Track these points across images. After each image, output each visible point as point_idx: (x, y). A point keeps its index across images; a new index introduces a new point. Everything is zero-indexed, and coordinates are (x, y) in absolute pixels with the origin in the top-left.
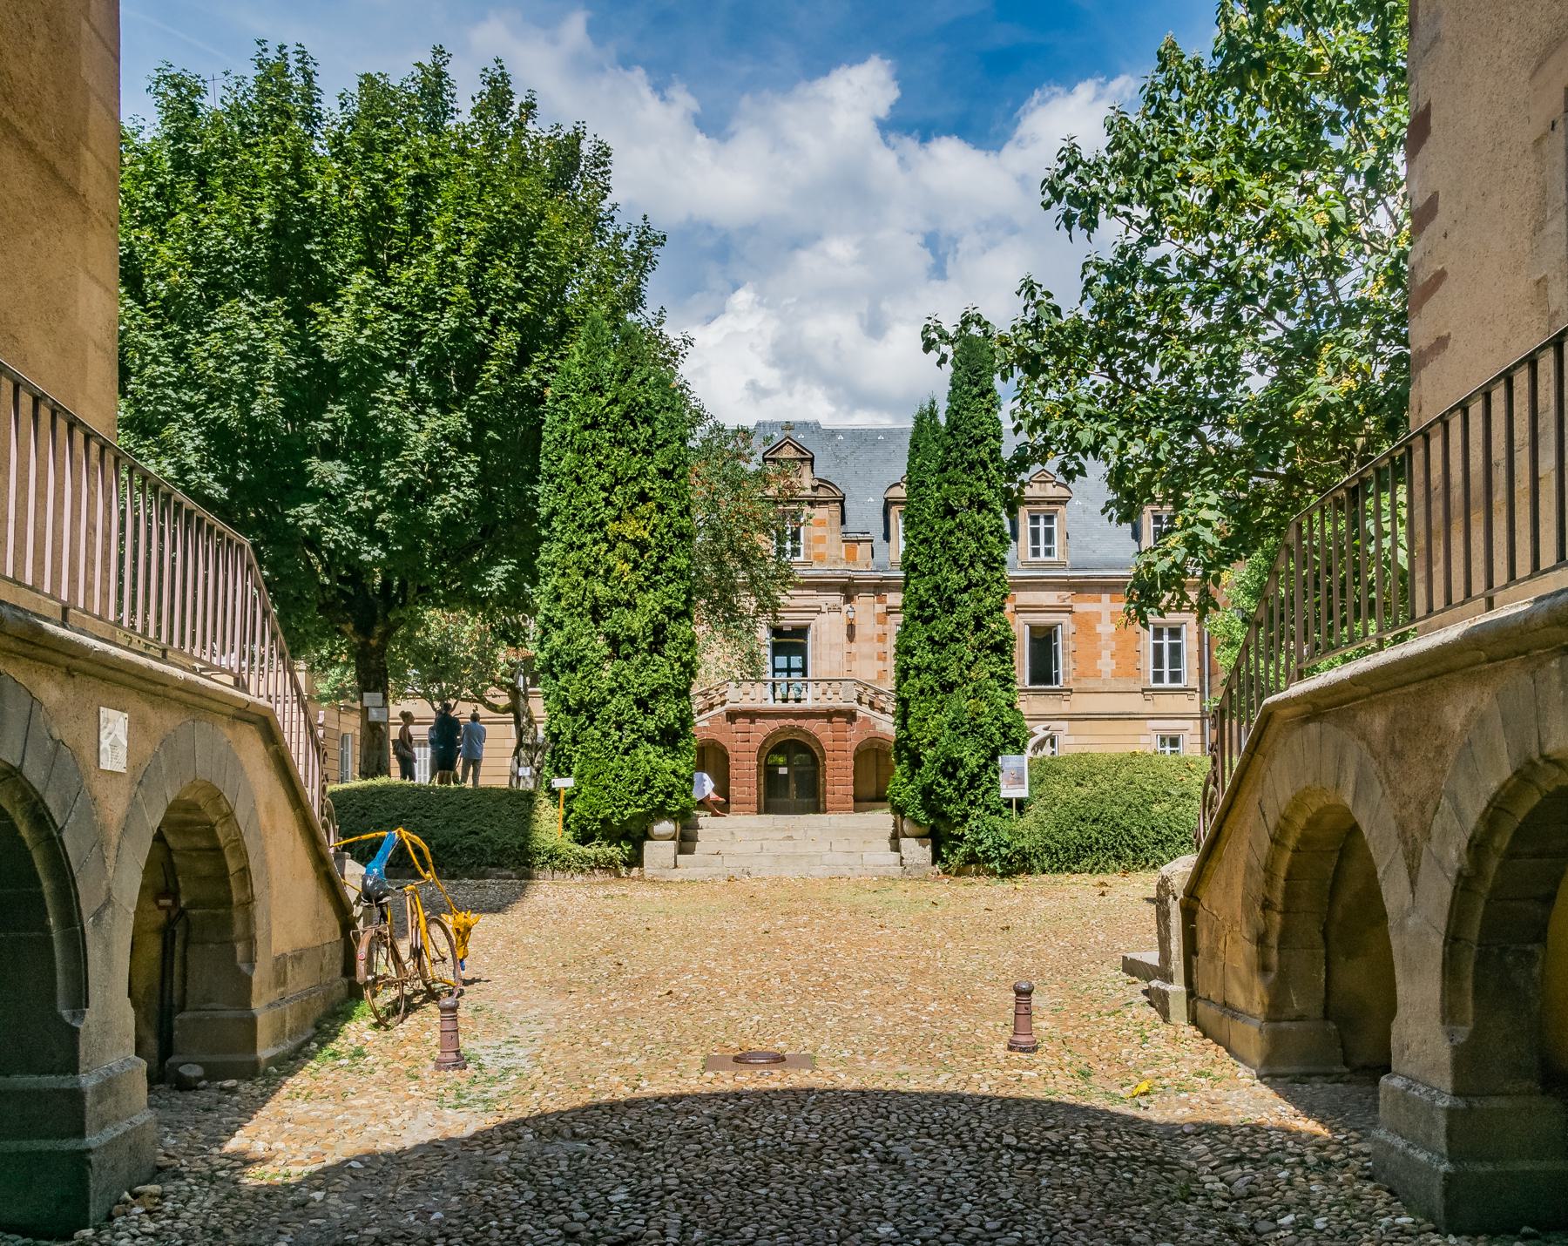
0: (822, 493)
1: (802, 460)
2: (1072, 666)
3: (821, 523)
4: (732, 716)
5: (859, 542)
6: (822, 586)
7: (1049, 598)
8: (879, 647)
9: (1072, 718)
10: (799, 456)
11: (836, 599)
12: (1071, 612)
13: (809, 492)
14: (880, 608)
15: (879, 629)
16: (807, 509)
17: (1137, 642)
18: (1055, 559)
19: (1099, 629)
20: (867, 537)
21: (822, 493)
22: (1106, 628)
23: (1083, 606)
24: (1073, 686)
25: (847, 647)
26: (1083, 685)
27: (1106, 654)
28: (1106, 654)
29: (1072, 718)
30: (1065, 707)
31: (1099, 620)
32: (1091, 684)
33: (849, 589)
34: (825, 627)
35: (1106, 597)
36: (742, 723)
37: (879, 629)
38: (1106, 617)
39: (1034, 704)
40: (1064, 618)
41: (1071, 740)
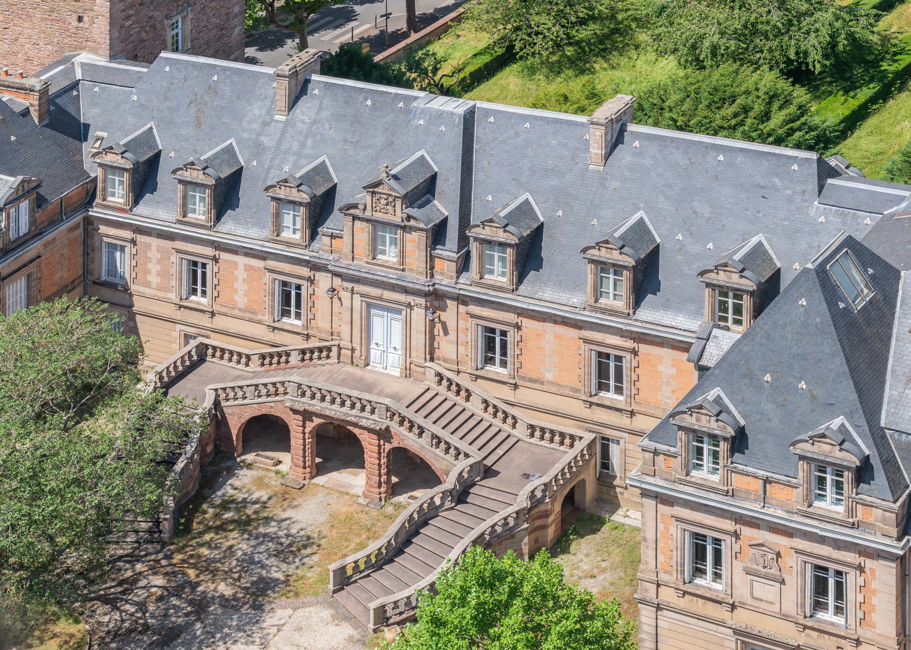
26: (642, 409)
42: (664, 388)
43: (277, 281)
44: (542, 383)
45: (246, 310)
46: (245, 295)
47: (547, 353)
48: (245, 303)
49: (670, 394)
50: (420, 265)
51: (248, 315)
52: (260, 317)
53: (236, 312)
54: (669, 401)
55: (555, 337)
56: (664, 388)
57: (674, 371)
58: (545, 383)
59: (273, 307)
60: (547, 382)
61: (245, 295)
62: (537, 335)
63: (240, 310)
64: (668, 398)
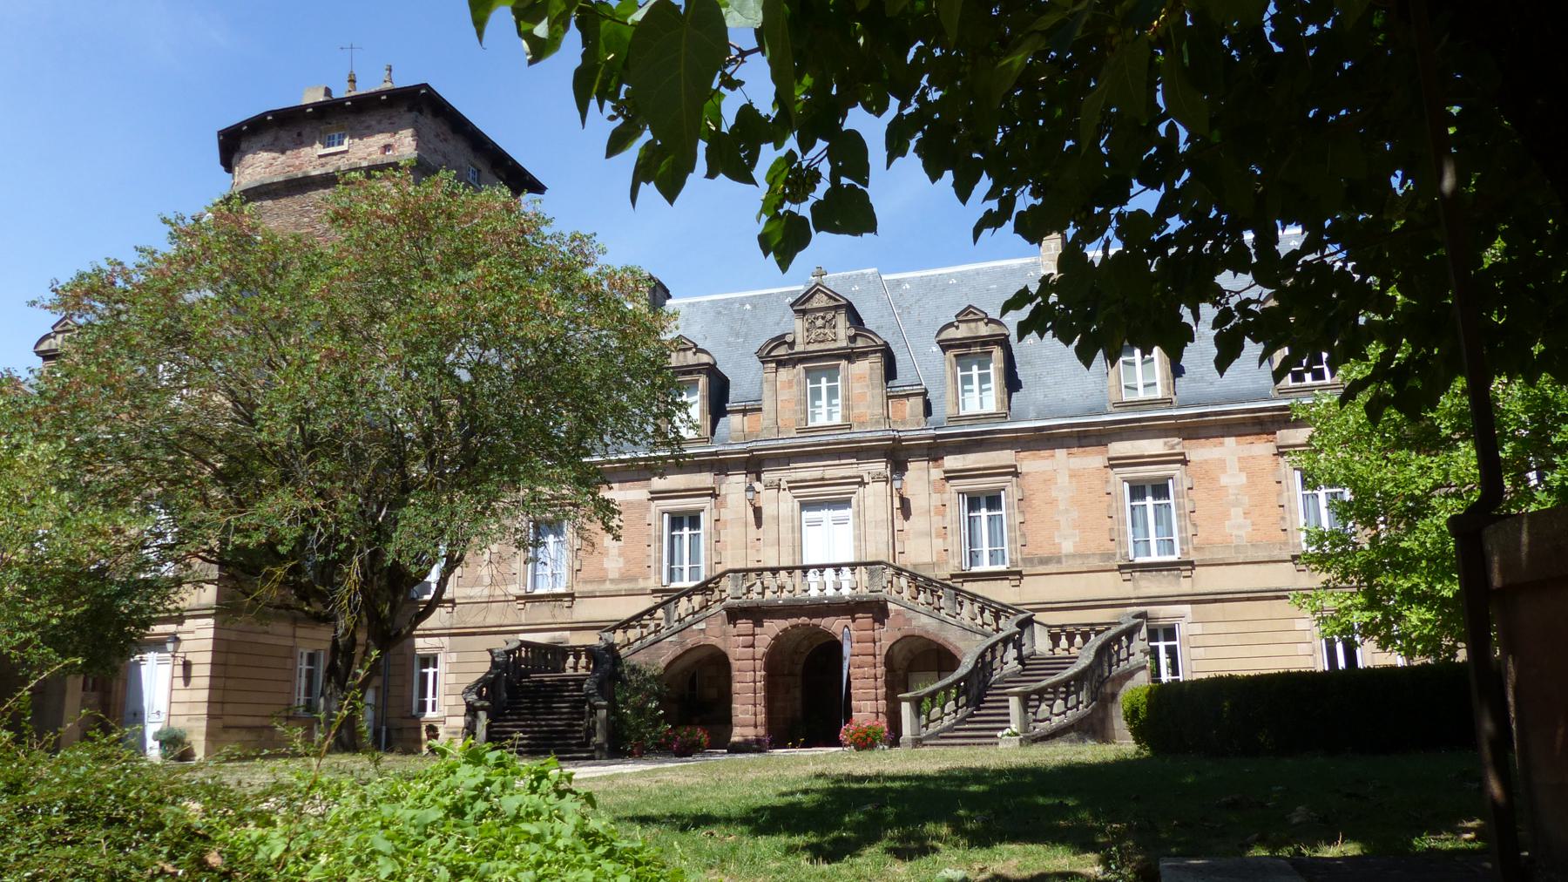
0: (860, 343)
1: (836, 308)
2: (1191, 531)
3: (861, 378)
4: (734, 614)
5: (908, 396)
6: (861, 452)
7: (1155, 446)
8: (937, 522)
9: (1196, 600)
10: (833, 303)
11: (880, 467)
12: (1185, 462)
13: (844, 344)
14: (937, 474)
15: (936, 499)
16: (843, 363)
17: (1279, 494)
18: (1159, 395)
19: (1224, 480)
20: (917, 389)
21: (860, 343)
22: (1233, 479)
23: (1202, 452)
24: (1193, 557)
25: (899, 523)
27: (1236, 513)
28: (1236, 513)
29: (1196, 600)
30: (1184, 586)
31: (1224, 470)
32: (1220, 556)
33: (897, 455)
34: (869, 501)
35: (1230, 442)
36: (745, 625)
37: (936, 499)
38: (1233, 464)
39: (1143, 583)
40: (1175, 470)
41: (1197, 628)
42: (1233, 510)
43: (666, 516)
44: (1059, 561)
45: (623, 579)
46: (620, 555)
47: (1061, 507)
48: (620, 569)
49: (1241, 520)
50: (875, 412)
51: (624, 586)
52: (641, 584)
53: (608, 586)
54: (1242, 533)
55: (1071, 476)
56: (1233, 511)
57: (1242, 479)
58: (1064, 560)
59: (660, 560)
60: (1066, 556)
61: (620, 555)
62: (1045, 481)
63: (612, 581)
64: (1240, 527)
